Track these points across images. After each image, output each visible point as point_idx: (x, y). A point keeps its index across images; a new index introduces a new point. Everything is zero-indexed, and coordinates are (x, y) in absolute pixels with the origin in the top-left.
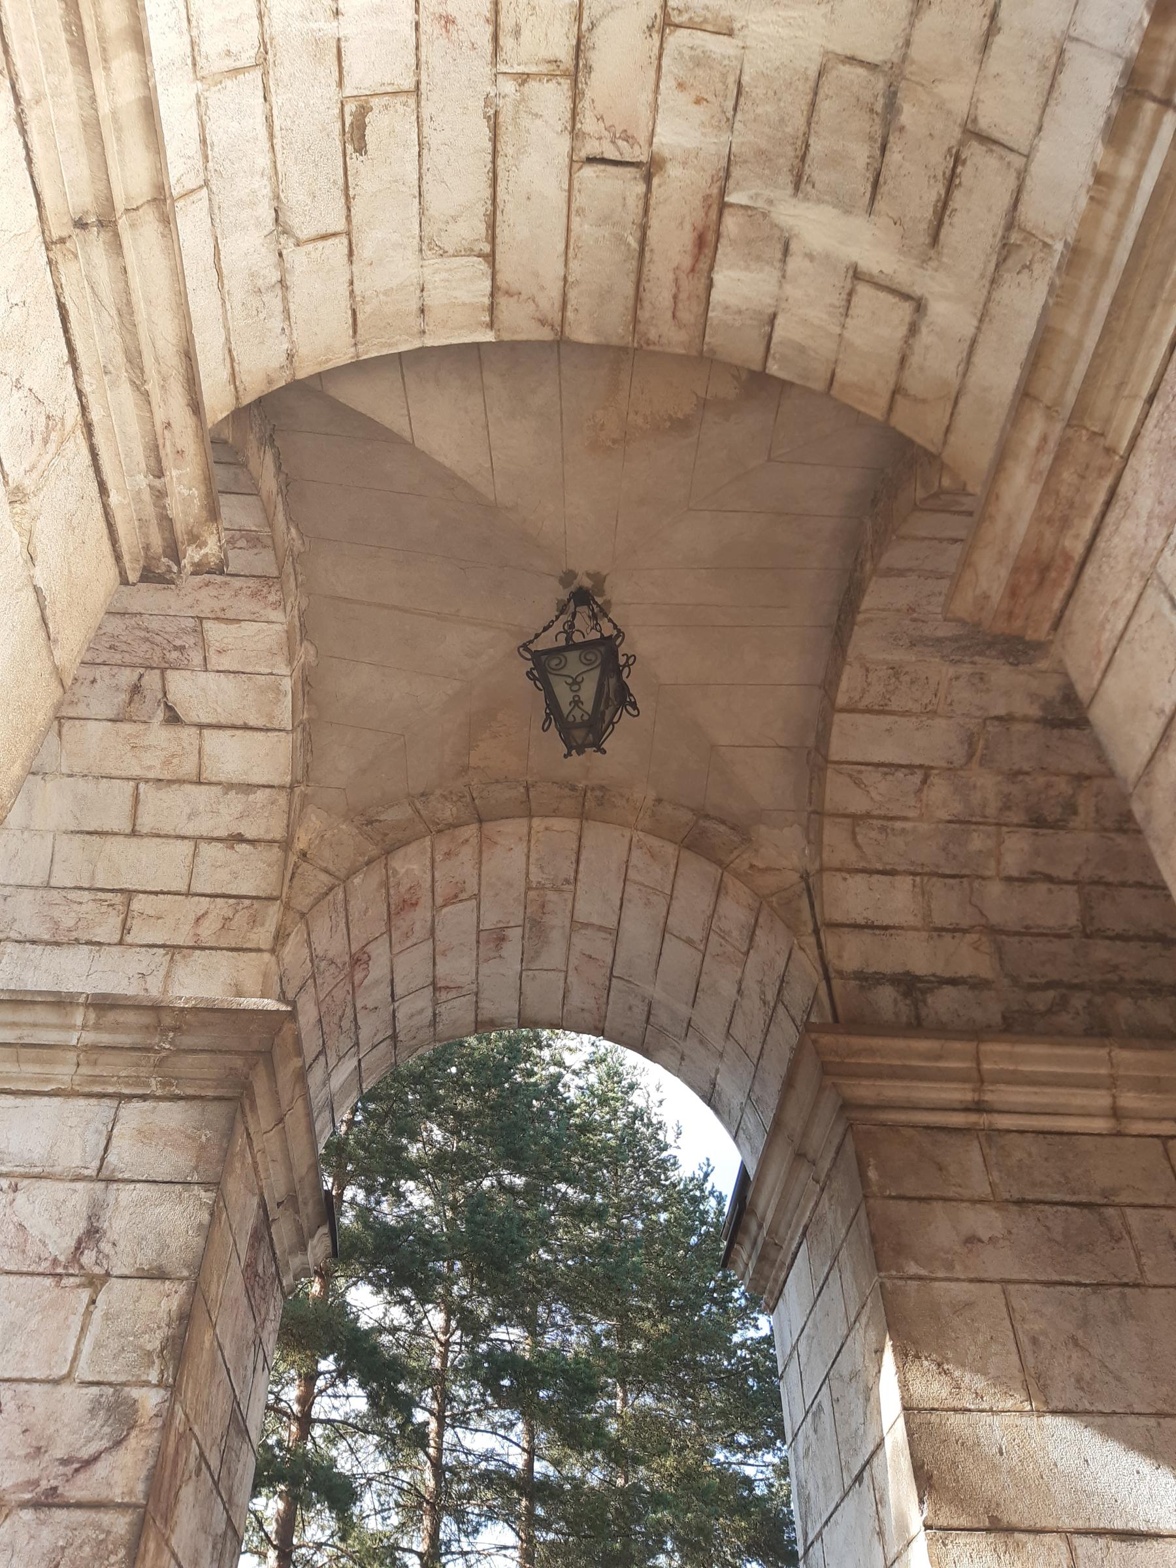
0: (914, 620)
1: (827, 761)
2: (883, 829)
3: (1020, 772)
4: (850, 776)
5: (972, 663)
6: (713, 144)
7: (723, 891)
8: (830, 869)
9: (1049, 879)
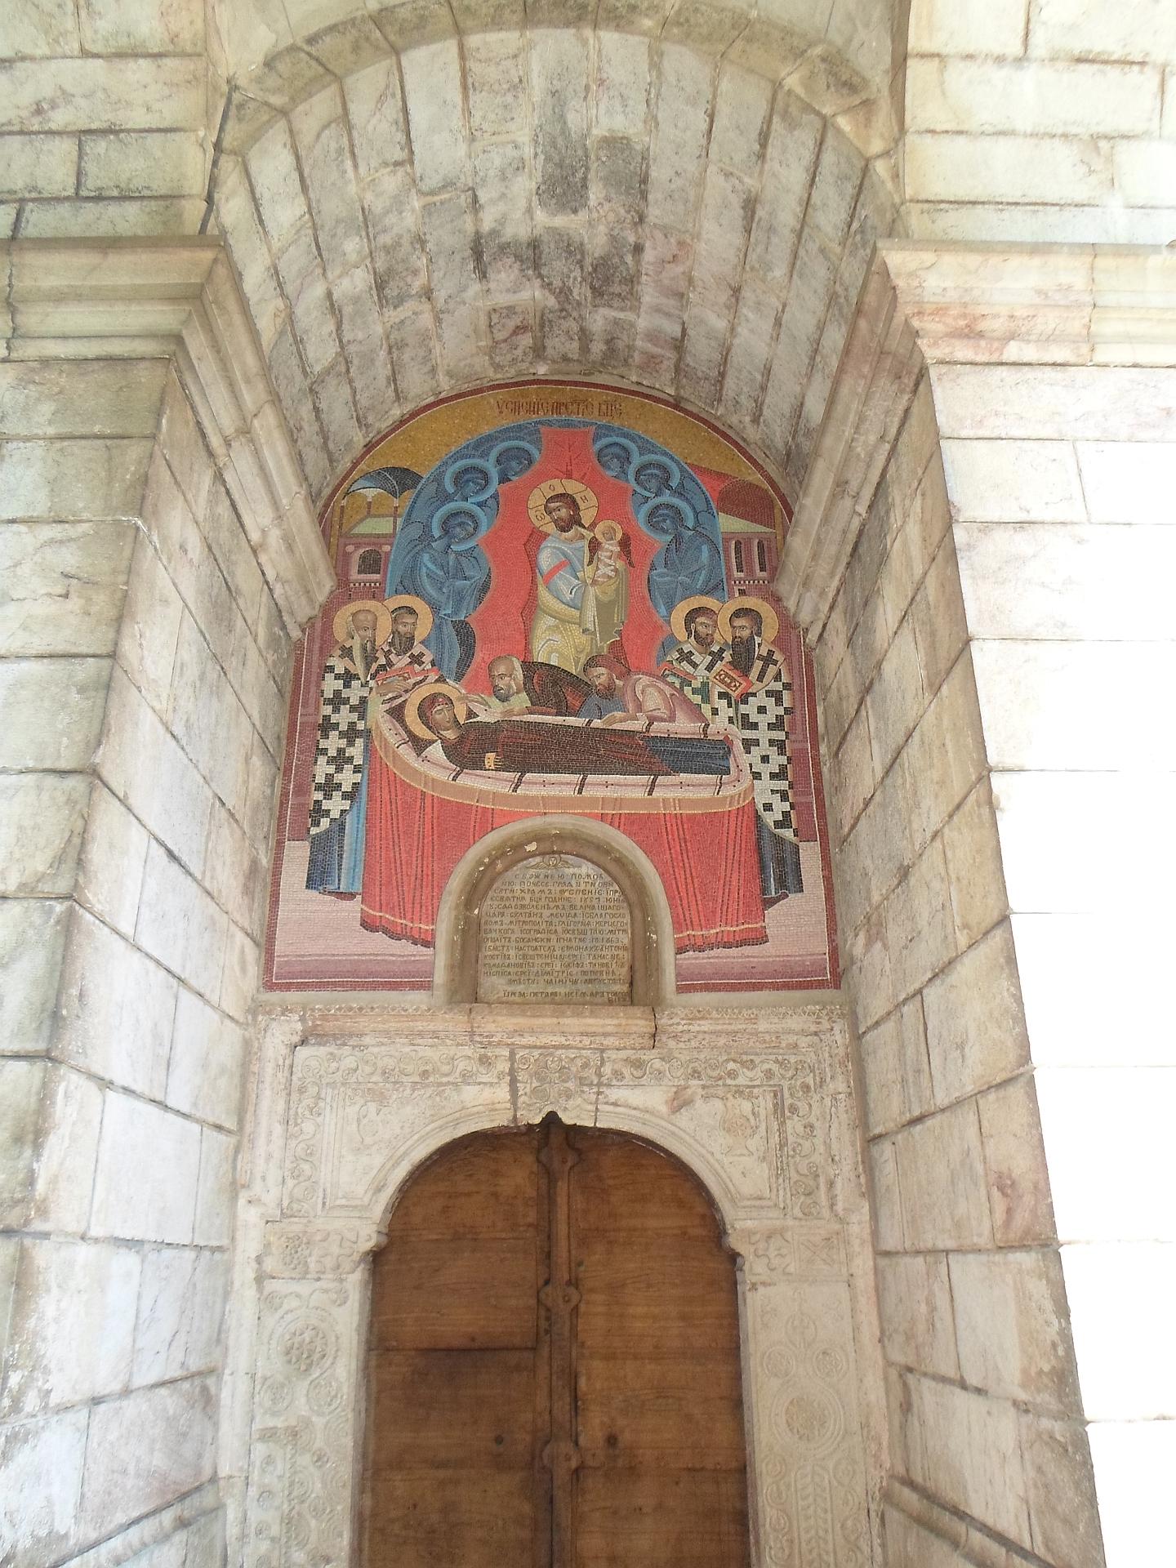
0: (587, 88)
1: (396, 51)
2: (340, 151)
4: (387, 87)
5: (536, 155)
8: (289, 122)
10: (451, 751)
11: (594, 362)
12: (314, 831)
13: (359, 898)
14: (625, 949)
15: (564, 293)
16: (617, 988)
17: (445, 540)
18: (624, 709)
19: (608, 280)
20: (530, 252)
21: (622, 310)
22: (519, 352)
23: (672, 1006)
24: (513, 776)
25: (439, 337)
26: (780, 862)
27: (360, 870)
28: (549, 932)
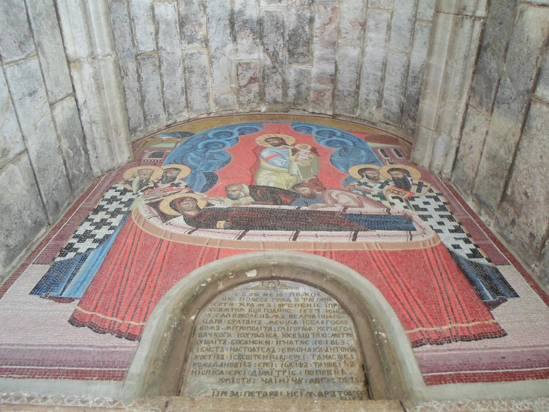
3: (205, 7)
9: (157, 33)
10: (188, 220)
11: (290, 103)
12: (58, 259)
13: (77, 301)
14: (353, 350)
15: (274, 56)
16: (350, 387)
17: (206, 149)
18: (324, 202)
19: (296, 44)
20: (258, 27)
21: (304, 63)
22: (251, 95)
23: (424, 400)
24: (240, 232)
25: (211, 74)
26: (486, 278)
27: (86, 284)
28: (269, 336)
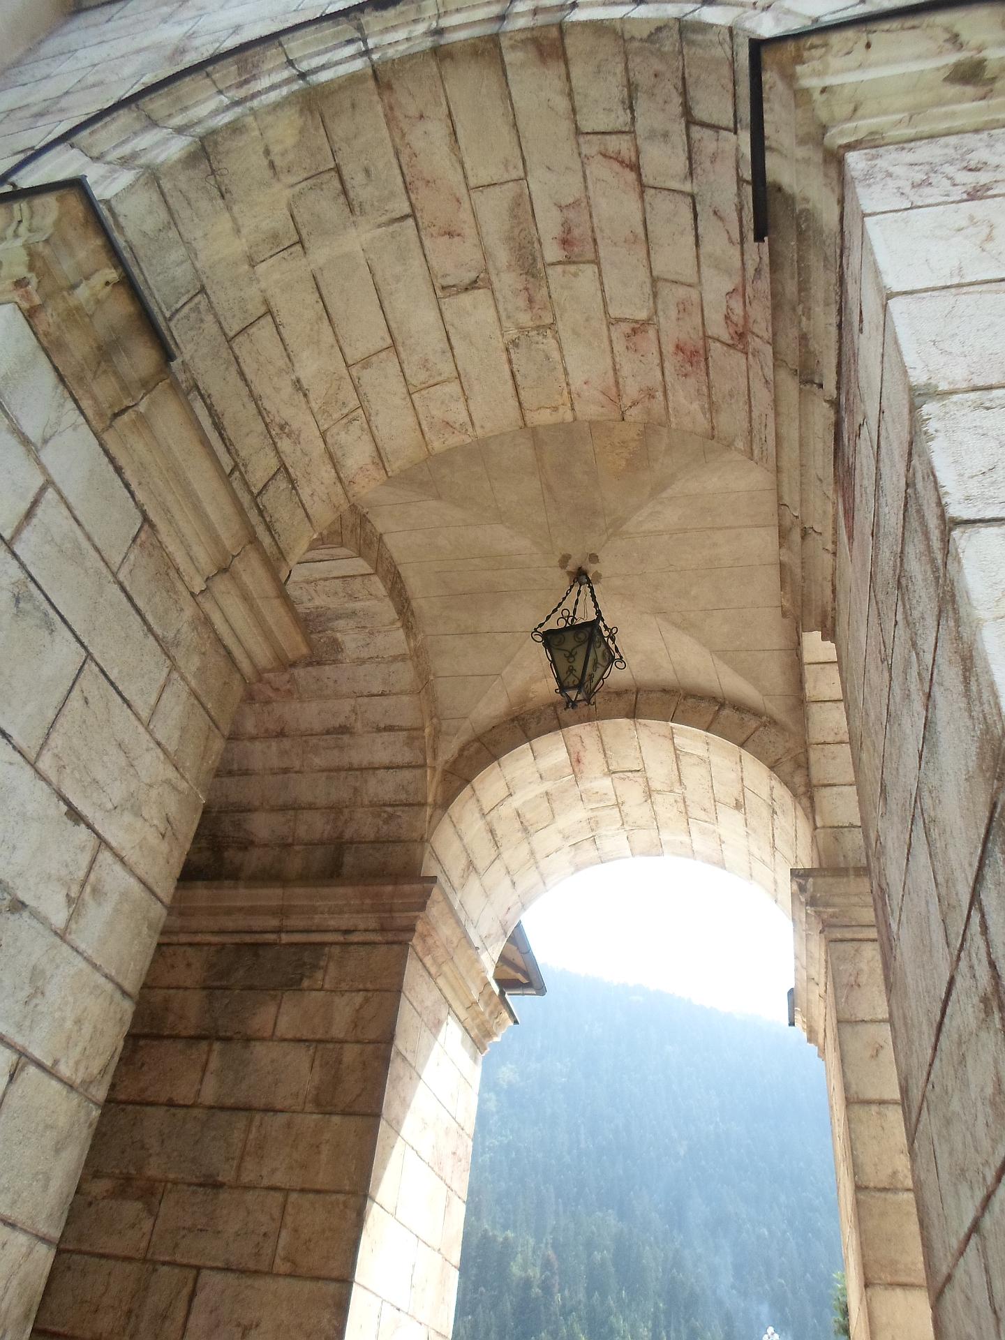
6: (585, 785)
7: (377, 460)
